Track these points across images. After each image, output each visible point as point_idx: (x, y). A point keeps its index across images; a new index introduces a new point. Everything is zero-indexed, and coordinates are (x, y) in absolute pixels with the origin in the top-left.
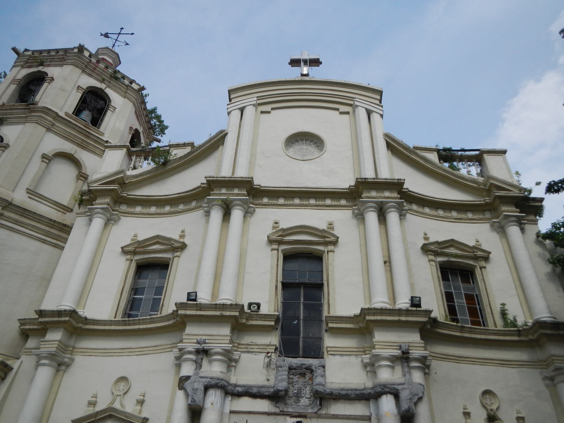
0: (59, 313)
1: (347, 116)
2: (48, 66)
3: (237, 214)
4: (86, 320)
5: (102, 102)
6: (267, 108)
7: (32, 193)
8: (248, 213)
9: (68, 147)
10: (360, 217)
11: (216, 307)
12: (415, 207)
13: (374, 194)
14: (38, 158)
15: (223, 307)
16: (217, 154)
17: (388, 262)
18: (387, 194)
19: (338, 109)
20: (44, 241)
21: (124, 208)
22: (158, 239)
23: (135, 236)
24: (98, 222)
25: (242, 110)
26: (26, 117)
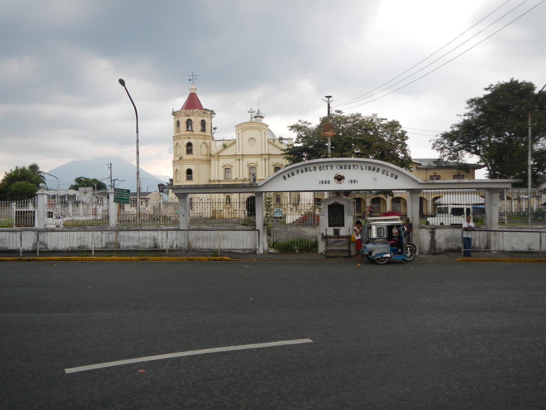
0: (217, 180)
1: (260, 132)
2: (190, 116)
3: (241, 161)
4: (220, 180)
5: (204, 122)
6: (244, 130)
7: (201, 155)
8: (242, 160)
9: (203, 141)
10: (262, 160)
11: (240, 180)
12: (272, 156)
13: (264, 156)
14: (200, 146)
15: (241, 180)
16: (235, 144)
17: (265, 169)
18: (266, 156)
19: (258, 130)
20: (207, 164)
21: (219, 157)
22: (227, 164)
23: (223, 163)
24: (216, 162)
25: (239, 133)
26: (194, 137)
